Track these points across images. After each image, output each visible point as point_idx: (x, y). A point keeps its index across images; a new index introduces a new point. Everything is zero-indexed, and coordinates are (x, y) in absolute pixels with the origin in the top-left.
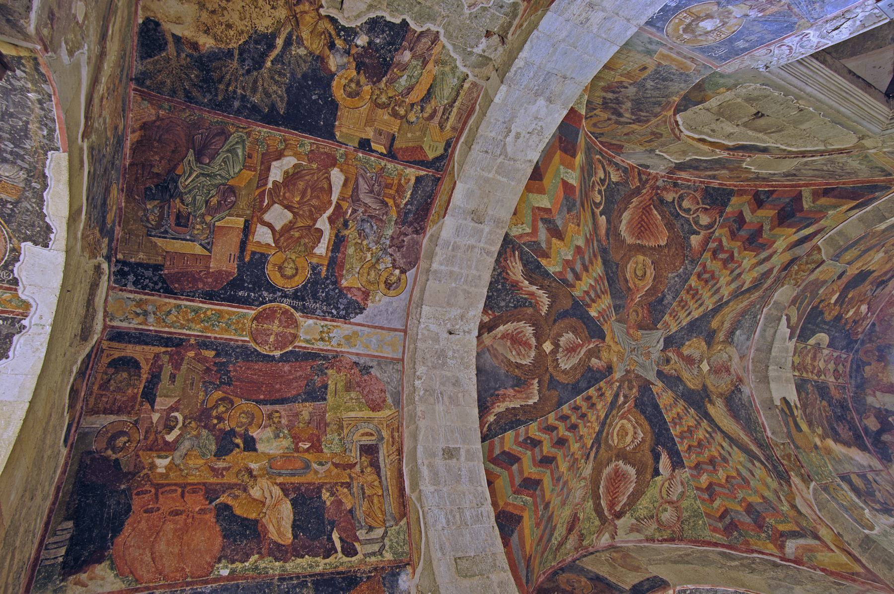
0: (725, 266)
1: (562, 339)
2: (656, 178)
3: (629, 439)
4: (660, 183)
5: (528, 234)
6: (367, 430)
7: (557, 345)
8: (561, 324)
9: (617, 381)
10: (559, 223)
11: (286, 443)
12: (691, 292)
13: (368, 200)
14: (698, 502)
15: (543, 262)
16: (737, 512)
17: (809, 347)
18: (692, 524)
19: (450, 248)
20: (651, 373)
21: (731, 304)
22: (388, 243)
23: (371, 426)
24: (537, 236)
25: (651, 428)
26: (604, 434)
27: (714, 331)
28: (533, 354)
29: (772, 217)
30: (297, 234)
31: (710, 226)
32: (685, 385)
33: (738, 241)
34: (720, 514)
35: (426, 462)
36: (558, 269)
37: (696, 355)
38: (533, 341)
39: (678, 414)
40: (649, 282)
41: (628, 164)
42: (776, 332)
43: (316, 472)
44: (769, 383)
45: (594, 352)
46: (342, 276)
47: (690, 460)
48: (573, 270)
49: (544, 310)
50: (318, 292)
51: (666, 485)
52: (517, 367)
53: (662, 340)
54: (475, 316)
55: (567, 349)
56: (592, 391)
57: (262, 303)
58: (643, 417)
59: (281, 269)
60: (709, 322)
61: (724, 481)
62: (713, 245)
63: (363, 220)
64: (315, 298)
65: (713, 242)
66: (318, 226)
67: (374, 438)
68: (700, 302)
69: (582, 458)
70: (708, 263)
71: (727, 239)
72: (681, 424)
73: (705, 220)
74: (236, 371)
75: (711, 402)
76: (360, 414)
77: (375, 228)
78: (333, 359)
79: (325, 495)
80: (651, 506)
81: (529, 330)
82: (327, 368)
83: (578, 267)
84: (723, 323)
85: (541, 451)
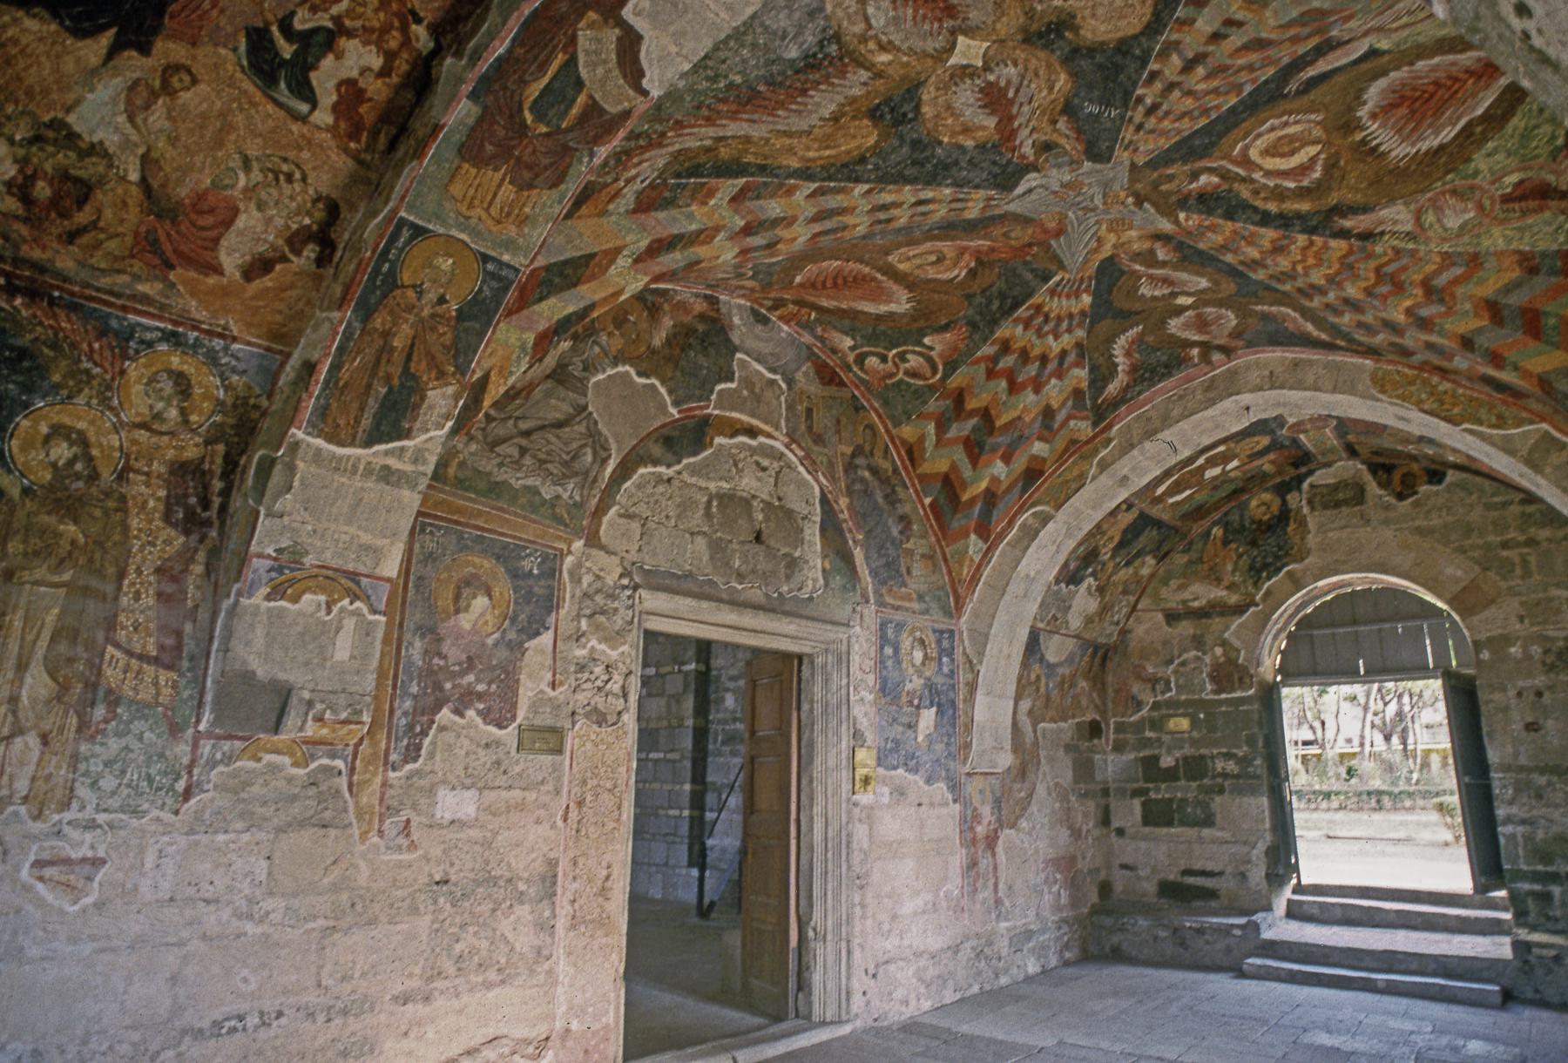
21: (795, 163)
27: (874, 114)
37: (966, 97)
53: (1019, 190)
68: (882, 216)
84: (835, 118)
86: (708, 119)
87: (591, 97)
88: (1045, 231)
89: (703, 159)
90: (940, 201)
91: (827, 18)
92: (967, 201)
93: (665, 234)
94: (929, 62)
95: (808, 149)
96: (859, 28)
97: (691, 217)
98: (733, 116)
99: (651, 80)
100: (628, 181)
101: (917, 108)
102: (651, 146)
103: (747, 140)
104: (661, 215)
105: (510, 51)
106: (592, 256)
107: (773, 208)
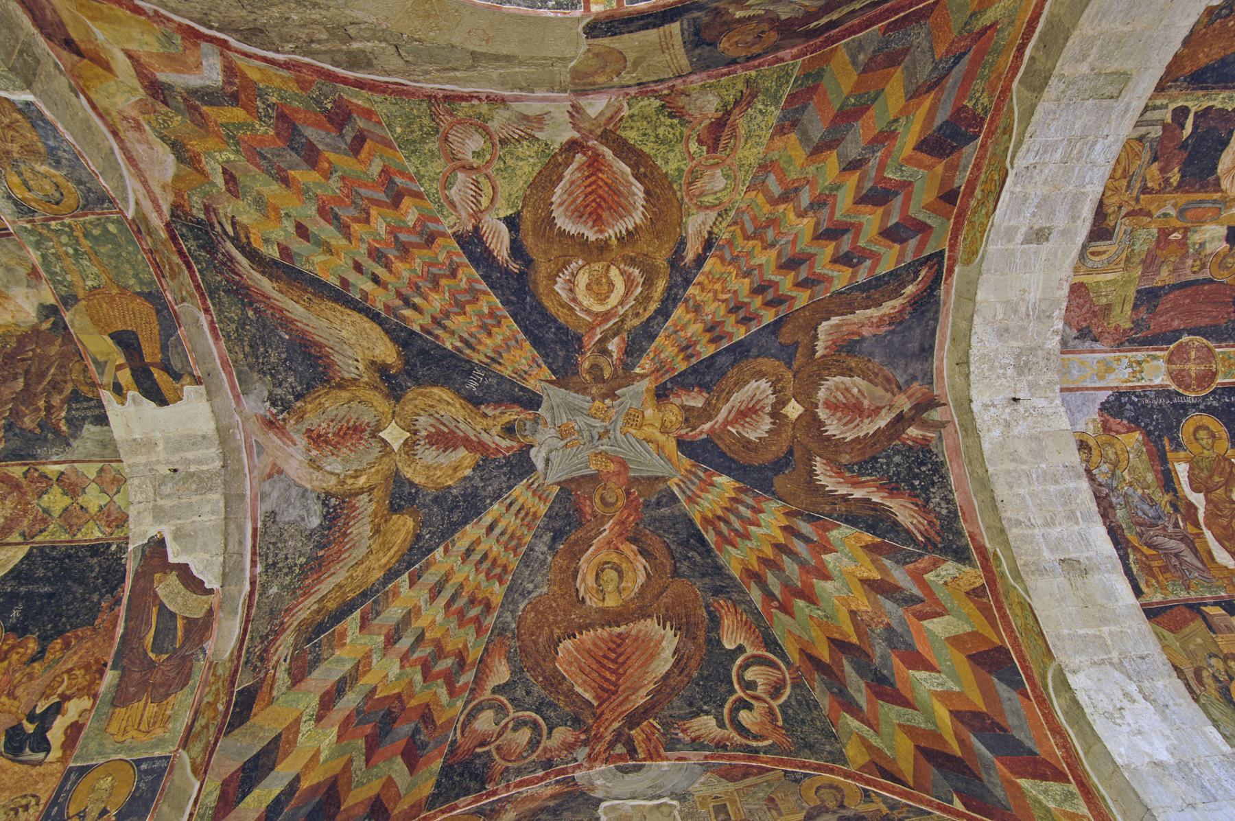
0: (438, 646)
1: (767, 427)
2: (592, 759)
3: (583, 279)
4: (582, 753)
5: (926, 571)
6: (1097, 259)
7: (776, 414)
8: (777, 450)
9: (643, 376)
10: (889, 605)
11: (1196, 238)
12: (498, 570)
13: (1172, 544)
14: (412, 170)
15: (868, 538)
16: (336, 150)
17: (15, 537)
18: (415, 127)
19: (1079, 514)
20: (556, 401)
22: (1113, 499)
23: (1090, 264)
24: (907, 571)
25: (540, 303)
26: (661, 284)
27: (395, 509)
28: (822, 394)
29: (349, 790)
30: (1216, 479)
31: (472, 716)
32: (457, 392)
33: (415, 708)
34: (366, 146)
35: (1079, 222)
36: (834, 535)
37: (428, 454)
38: (822, 413)
39: (490, 334)
40: (587, 565)
41: (667, 759)
42: (226, 545)
43: (1174, 205)
44: (218, 429)
45: (699, 417)
46: (1144, 444)
47: (447, 251)
48: (807, 540)
49: (819, 465)
50: (1163, 418)
51: (485, 202)
52: (851, 370)
53: (540, 465)
54: (989, 430)
55: (756, 412)
56: (706, 350)
57: (1213, 392)
58: (561, 320)
59: (1213, 436)
60: (424, 524)
61: (374, 212)
62: (467, 677)
63: (1160, 518)
64: (1161, 409)
65: (466, 684)
66: (1201, 495)
67: (1091, 249)
68: (476, 557)
69: (730, 242)
70: (471, 638)
71: (438, 703)
72: (480, 315)
73: (485, 722)
74: (1228, 313)
75: (381, 369)
76: (1100, 278)
77: (1140, 514)
78: (1124, 341)
79: (1175, 178)
80: (510, 162)
81: (833, 428)
82: (1131, 329)
83: (800, 547)
84: (377, 531)
85: (837, 248)
86: (305, 594)
87: (185, 618)
88: (618, 474)
89: (319, 618)
90: (501, 516)
91: (313, 491)
92: (516, 500)
93: (328, 685)
94: (386, 460)
95: (379, 560)
96: (334, 480)
97: (339, 661)
98: (319, 581)
99: (210, 582)
100: (275, 668)
101: (412, 484)
102: (277, 634)
103: (339, 586)
104: (316, 674)
105: (126, 628)
106: (280, 735)
107: (394, 612)
